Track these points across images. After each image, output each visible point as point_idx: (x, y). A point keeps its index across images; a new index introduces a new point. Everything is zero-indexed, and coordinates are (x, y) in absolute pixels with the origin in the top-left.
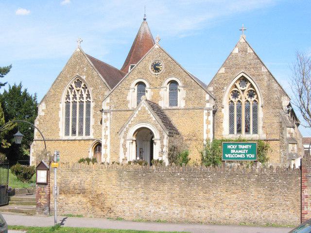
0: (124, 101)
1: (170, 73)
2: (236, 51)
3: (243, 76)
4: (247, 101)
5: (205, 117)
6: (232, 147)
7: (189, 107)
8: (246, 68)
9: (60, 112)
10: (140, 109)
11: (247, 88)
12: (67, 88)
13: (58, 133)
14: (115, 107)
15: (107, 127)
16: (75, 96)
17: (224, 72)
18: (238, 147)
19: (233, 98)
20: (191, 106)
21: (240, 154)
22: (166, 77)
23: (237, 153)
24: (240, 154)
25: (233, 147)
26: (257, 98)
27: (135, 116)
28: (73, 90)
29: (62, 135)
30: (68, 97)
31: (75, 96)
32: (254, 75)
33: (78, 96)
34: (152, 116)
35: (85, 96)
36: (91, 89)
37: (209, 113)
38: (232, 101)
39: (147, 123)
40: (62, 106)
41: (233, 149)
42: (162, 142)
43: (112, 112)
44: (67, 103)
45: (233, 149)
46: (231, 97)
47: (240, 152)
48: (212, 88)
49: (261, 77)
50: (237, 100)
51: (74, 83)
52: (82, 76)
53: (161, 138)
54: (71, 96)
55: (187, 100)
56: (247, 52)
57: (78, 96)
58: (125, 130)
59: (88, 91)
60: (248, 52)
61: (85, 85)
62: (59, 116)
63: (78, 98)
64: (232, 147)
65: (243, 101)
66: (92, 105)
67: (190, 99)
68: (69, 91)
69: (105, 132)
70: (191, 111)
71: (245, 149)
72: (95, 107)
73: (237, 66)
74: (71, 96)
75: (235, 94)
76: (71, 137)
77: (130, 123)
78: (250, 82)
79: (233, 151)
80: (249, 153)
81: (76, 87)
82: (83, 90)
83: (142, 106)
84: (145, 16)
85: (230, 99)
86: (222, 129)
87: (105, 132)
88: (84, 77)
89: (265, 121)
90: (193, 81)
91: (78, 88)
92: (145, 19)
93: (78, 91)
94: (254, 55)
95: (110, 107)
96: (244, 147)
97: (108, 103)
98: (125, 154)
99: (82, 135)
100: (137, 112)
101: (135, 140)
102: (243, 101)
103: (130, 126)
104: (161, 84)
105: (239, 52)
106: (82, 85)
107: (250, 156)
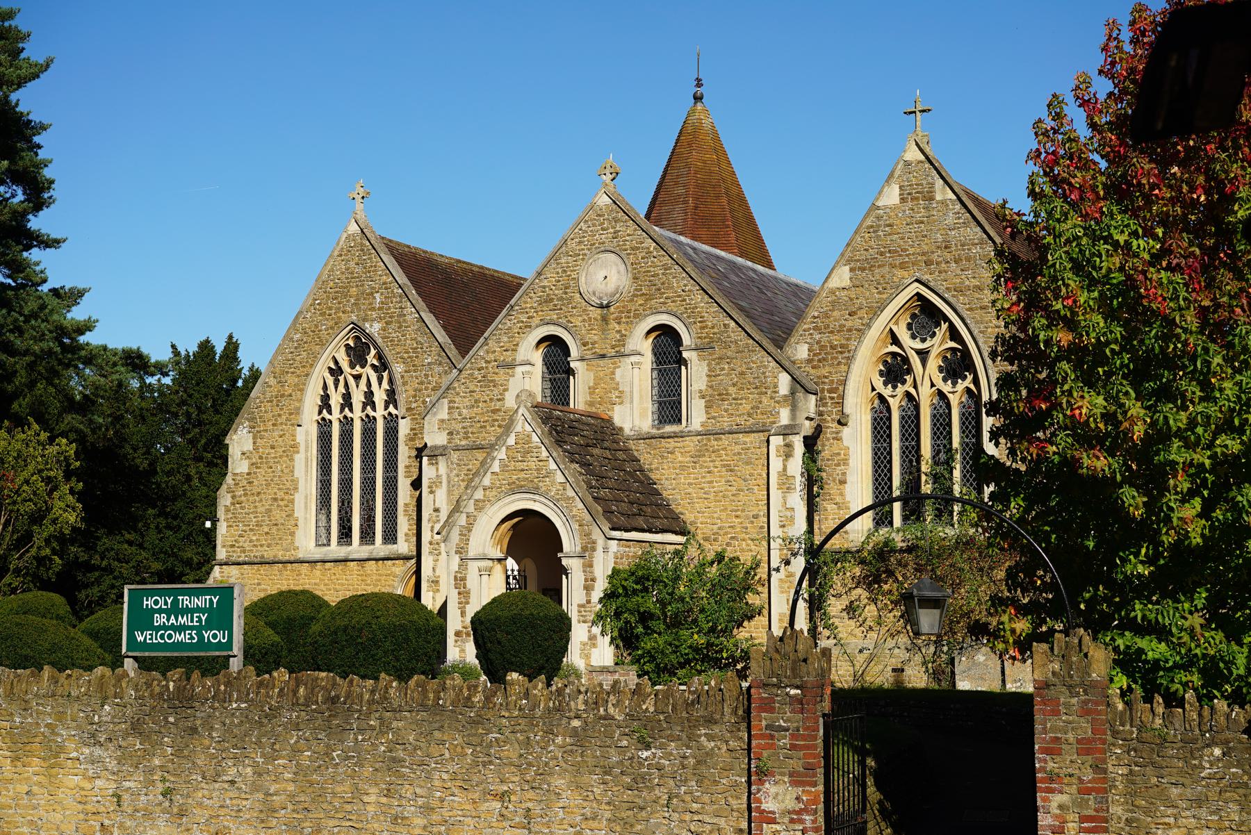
0: (494, 411)
1: (649, 298)
2: (891, 196)
3: (919, 296)
4: (941, 394)
5: (776, 464)
6: (156, 602)
7: (717, 428)
9: (297, 457)
10: (511, 441)
11: (939, 343)
12: (320, 372)
13: (293, 534)
15: (437, 510)
16: (347, 401)
17: (847, 283)
18: (175, 602)
19: (945, 380)
20: (726, 423)
21: (181, 629)
22: (637, 316)
23: (173, 627)
24: (181, 629)
25: (161, 602)
26: (976, 381)
27: (496, 467)
29: (306, 544)
30: (325, 404)
31: (347, 401)
32: (959, 290)
33: (358, 398)
34: (553, 466)
35: (380, 396)
36: (398, 368)
37: (789, 446)
39: (535, 491)
40: (307, 434)
41: (160, 611)
42: (589, 566)
43: (455, 456)
44: (324, 426)
45: (160, 611)
46: (879, 382)
47: (183, 620)
48: (806, 347)
50: (901, 389)
51: (343, 349)
52: (367, 325)
53: (584, 549)
54: (336, 400)
55: (714, 398)
56: (932, 199)
57: (358, 398)
58: (462, 520)
60: (938, 197)
61: (380, 357)
62: (296, 474)
63: (380, 404)
64: (156, 602)
66: (404, 427)
67: (723, 396)
68: (330, 381)
71: (198, 609)
72: (411, 438)
73: (896, 257)
74: (336, 400)
75: (896, 370)
76: (336, 549)
77: (479, 494)
78: (946, 319)
79: (160, 619)
80: (209, 626)
81: (352, 366)
82: (374, 377)
83: (518, 428)
84: (699, 83)
85: (873, 389)
88: (374, 328)
90: (733, 324)
92: (698, 98)
93: (357, 378)
94: (958, 206)
95: (451, 434)
96: (198, 602)
97: (443, 421)
99: (373, 543)
100: (502, 454)
103: (480, 506)
104: (623, 339)
105: (903, 200)
106: (371, 358)
107: (215, 636)
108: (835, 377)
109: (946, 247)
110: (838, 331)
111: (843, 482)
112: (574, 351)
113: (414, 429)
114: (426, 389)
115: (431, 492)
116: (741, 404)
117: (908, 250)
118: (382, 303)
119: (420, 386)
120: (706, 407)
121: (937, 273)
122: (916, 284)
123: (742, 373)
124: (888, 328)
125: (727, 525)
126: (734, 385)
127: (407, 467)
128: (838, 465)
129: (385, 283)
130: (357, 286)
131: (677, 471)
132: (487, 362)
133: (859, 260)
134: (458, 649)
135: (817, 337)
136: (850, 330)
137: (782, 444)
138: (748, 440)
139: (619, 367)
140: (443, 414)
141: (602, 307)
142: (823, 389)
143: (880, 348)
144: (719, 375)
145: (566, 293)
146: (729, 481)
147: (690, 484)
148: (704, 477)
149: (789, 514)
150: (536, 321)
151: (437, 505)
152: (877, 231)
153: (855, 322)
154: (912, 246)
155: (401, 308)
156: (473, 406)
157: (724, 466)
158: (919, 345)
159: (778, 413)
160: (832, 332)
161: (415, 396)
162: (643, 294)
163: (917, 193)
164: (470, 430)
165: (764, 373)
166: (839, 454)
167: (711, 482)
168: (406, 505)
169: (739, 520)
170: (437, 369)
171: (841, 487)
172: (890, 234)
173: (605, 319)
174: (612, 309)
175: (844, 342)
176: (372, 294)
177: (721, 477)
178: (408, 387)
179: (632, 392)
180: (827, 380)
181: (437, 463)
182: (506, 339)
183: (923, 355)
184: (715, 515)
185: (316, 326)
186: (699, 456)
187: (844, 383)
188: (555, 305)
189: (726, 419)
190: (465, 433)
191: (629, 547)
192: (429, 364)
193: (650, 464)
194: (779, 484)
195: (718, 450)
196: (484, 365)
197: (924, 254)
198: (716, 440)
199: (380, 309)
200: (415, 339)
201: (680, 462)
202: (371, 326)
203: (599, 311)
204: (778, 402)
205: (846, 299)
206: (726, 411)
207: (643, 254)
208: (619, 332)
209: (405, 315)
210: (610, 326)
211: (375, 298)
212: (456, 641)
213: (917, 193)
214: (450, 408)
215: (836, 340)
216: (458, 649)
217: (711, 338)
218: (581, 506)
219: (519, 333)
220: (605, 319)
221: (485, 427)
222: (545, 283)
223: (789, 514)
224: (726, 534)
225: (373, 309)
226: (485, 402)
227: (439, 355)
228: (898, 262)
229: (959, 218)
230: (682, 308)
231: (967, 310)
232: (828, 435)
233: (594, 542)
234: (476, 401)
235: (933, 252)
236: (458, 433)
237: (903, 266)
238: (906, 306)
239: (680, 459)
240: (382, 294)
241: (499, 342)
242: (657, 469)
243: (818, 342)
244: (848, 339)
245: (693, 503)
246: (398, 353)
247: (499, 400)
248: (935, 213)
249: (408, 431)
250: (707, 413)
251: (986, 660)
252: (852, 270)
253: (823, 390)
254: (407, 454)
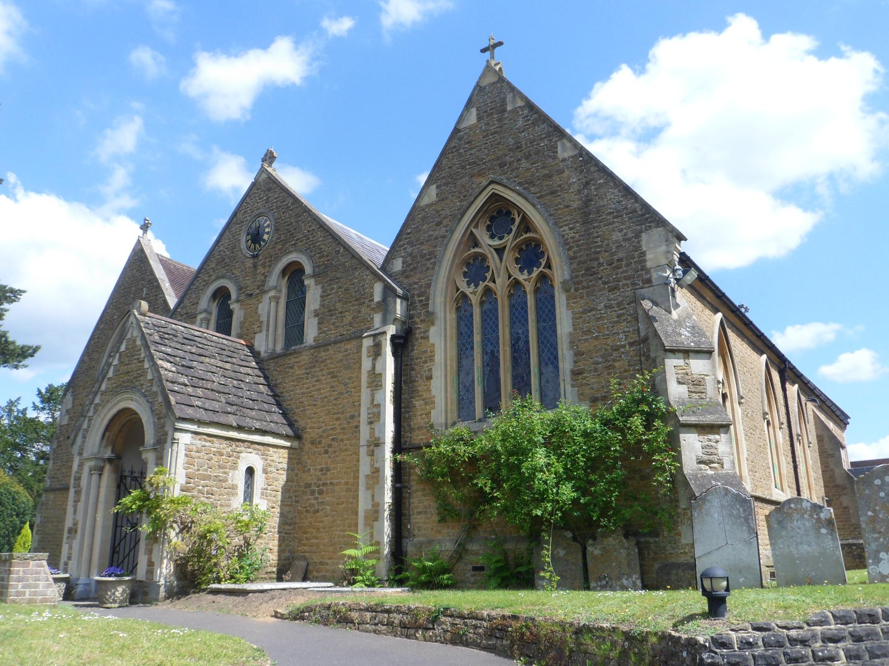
1: (285, 242)
4: (517, 284)
8: (502, 165)
20: (333, 335)
26: (549, 266)
38: (464, 296)
49: (557, 180)
56: (505, 110)
60: (509, 108)
65: (500, 286)
67: (331, 312)
70: (331, 350)
78: (520, 210)
85: (458, 289)
86: (430, 402)
89: (583, 347)
101: (110, 460)
102: (500, 286)
108: (423, 282)
109: (518, 148)
110: (427, 241)
111: (430, 378)
116: (345, 316)
117: (483, 159)
120: (319, 323)
121: (509, 172)
123: (347, 289)
124: (469, 232)
125: (329, 428)
126: (339, 301)
128: (426, 362)
131: (295, 383)
133: (444, 177)
135: (409, 250)
136: (436, 238)
137: (372, 344)
138: (348, 347)
142: (414, 294)
143: (464, 251)
144: (329, 295)
146: (332, 387)
147: (303, 393)
148: (314, 386)
149: (375, 410)
152: (459, 150)
153: (442, 231)
154: (488, 155)
157: (329, 374)
158: (496, 242)
159: (372, 318)
160: (422, 243)
163: (491, 109)
165: (363, 286)
166: (426, 352)
167: (319, 390)
169: (339, 422)
171: (427, 383)
172: (469, 150)
173: (255, 266)
174: (260, 258)
175: (432, 249)
177: (327, 383)
179: (268, 321)
180: (416, 286)
183: (500, 251)
184: (321, 420)
186: (311, 368)
187: (429, 286)
189: (333, 332)
191: (212, 442)
193: (276, 380)
194: (369, 383)
195: (325, 360)
197: (498, 158)
198: (324, 351)
201: (297, 375)
204: (373, 309)
205: (433, 212)
206: (333, 324)
207: (283, 210)
208: (263, 274)
210: (258, 271)
213: (491, 109)
215: (425, 249)
217: (326, 265)
223: (375, 410)
224: (329, 435)
228: (475, 171)
229: (528, 120)
230: (307, 245)
231: (538, 198)
232: (417, 336)
233: (166, 434)
235: (506, 155)
237: (480, 174)
238: (485, 208)
239: (298, 372)
242: (281, 383)
243: (411, 254)
244: (435, 246)
245: (305, 411)
248: (506, 122)
250: (319, 329)
251: (566, 554)
252: (437, 187)
253: (413, 296)
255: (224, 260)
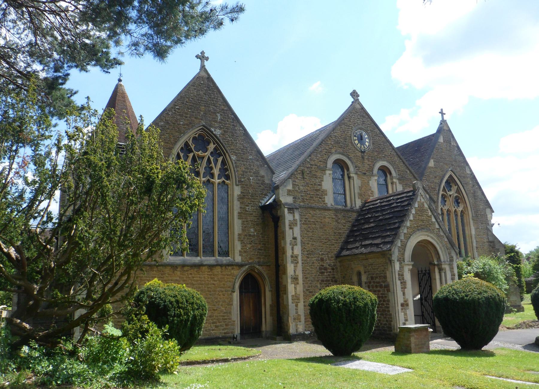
0: (317, 190)
14: (303, 202)
15: (295, 238)
28: (191, 155)
34: (434, 220)
35: (216, 172)
56: (451, 144)
59: (224, 163)
60: (452, 144)
61: (215, 149)
69: (293, 249)
78: (456, 184)
83: (418, 200)
87: (293, 249)
88: (218, 132)
91: (200, 153)
97: (289, 191)
98: (404, 294)
106: (211, 147)
112: (352, 169)
113: (243, 193)
114: (250, 172)
115: (291, 228)
118: (222, 120)
119: (246, 170)
122: (451, 172)
127: (239, 213)
129: (223, 110)
130: (205, 106)
132: (311, 165)
134: (403, 313)
139: (370, 180)
140: (290, 187)
141: (362, 152)
145: (346, 142)
150: (333, 151)
151: (295, 236)
155: (233, 125)
156: (306, 186)
161: (243, 175)
162: (377, 151)
164: (305, 198)
168: (239, 235)
170: (256, 163)
174: (365, 154)
176: (215, 113)
178: (239, 169)
181: (294, 213)
182: (319, 156)
185: (176, 121)
188: (342, 146)
190: (303, 199)
192: (251, 159)
196: (310, 166)
197: (451, 162)
199: (220, 122)
200: (242, 144)
202: (215, 131)
203: (360, 154)
209: (236, 130)
211: (217, 116)
212: (402, 309)
214: (293, 185)
216: (403, 313)
218: (446, 240)
219: (325, 155)
220: (363, 158)
221: (312, 197)
222: (336, 134)
225: (216, 121)
226: (312, 185)
227: (257, 156)
234: (307, 183)
236: (299, 198)
240: (221, 115)
241: (317, 157)
246: (232, 149)
247: (319, 185)
249: (239, 193)
254: (239, 206)
255: (339, 143)
